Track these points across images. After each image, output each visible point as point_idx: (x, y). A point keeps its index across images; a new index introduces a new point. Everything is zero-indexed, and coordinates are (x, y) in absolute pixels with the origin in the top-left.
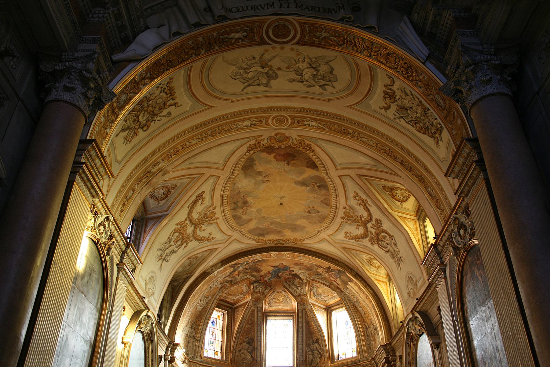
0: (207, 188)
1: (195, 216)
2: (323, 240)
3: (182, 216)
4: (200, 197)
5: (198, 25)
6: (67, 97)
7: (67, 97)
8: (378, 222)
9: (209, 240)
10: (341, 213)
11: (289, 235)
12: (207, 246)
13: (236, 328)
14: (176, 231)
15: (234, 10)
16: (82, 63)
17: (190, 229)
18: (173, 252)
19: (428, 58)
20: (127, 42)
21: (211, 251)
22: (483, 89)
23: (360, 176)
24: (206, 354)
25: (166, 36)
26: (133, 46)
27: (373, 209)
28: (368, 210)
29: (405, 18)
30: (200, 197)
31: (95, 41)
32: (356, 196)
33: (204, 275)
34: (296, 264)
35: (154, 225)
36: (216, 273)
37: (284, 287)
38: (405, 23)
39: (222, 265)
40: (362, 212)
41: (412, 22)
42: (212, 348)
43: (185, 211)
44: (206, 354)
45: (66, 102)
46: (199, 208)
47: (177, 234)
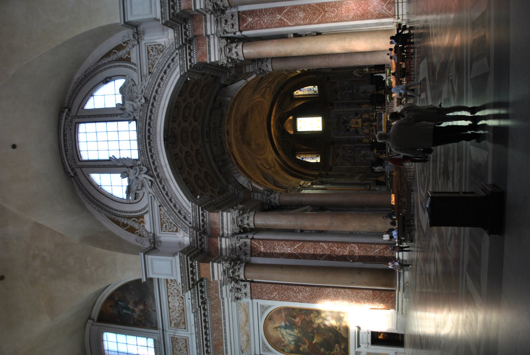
0: (258, 162)
1: (268, 167)
2: (268, 105)
3: (270, 172)
4: (262, 164)
5: (233, 164)
6: (277, 198)
7: (277, 198)
8: (269, 83)
9: (273, 162)
10: (261, 99)
11: (265, 124)
12: (275, 161)
13: (304, 147)
14: (276, 175)
15: (223, 151)
16: (264, 196)
17: (273, 169)
18: (283, 176)
19: (246, 80)
20: (244, 187)
21: (276, 160)
22: (269, 67)
23: (253, 93)
24: (319, 161)
25: (238, 174)
26: (245, 185)
27: (264, 86)
28: (264, 87)
29: (228, 87)
30: (262, 164)
31: (253, 195)
32: (258, 94)
33: (285, 163)
34: (275, 117)
35: (278, 183)
36: (283, 158)
37: (284, 123)
38: (230, 87)
39: (279, 155)
40: (263, 91)
41: (230, 85)
42: (315, 159)
43: (268, 171)
44: (319, 161)
45: (279, 198)
46: (265, 165)
47: (277, 174)
